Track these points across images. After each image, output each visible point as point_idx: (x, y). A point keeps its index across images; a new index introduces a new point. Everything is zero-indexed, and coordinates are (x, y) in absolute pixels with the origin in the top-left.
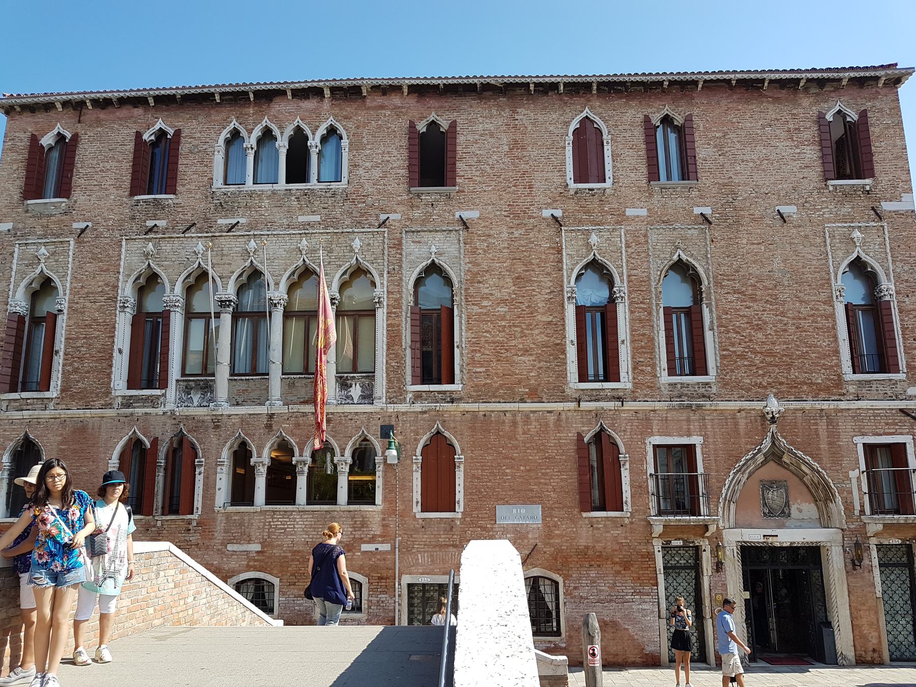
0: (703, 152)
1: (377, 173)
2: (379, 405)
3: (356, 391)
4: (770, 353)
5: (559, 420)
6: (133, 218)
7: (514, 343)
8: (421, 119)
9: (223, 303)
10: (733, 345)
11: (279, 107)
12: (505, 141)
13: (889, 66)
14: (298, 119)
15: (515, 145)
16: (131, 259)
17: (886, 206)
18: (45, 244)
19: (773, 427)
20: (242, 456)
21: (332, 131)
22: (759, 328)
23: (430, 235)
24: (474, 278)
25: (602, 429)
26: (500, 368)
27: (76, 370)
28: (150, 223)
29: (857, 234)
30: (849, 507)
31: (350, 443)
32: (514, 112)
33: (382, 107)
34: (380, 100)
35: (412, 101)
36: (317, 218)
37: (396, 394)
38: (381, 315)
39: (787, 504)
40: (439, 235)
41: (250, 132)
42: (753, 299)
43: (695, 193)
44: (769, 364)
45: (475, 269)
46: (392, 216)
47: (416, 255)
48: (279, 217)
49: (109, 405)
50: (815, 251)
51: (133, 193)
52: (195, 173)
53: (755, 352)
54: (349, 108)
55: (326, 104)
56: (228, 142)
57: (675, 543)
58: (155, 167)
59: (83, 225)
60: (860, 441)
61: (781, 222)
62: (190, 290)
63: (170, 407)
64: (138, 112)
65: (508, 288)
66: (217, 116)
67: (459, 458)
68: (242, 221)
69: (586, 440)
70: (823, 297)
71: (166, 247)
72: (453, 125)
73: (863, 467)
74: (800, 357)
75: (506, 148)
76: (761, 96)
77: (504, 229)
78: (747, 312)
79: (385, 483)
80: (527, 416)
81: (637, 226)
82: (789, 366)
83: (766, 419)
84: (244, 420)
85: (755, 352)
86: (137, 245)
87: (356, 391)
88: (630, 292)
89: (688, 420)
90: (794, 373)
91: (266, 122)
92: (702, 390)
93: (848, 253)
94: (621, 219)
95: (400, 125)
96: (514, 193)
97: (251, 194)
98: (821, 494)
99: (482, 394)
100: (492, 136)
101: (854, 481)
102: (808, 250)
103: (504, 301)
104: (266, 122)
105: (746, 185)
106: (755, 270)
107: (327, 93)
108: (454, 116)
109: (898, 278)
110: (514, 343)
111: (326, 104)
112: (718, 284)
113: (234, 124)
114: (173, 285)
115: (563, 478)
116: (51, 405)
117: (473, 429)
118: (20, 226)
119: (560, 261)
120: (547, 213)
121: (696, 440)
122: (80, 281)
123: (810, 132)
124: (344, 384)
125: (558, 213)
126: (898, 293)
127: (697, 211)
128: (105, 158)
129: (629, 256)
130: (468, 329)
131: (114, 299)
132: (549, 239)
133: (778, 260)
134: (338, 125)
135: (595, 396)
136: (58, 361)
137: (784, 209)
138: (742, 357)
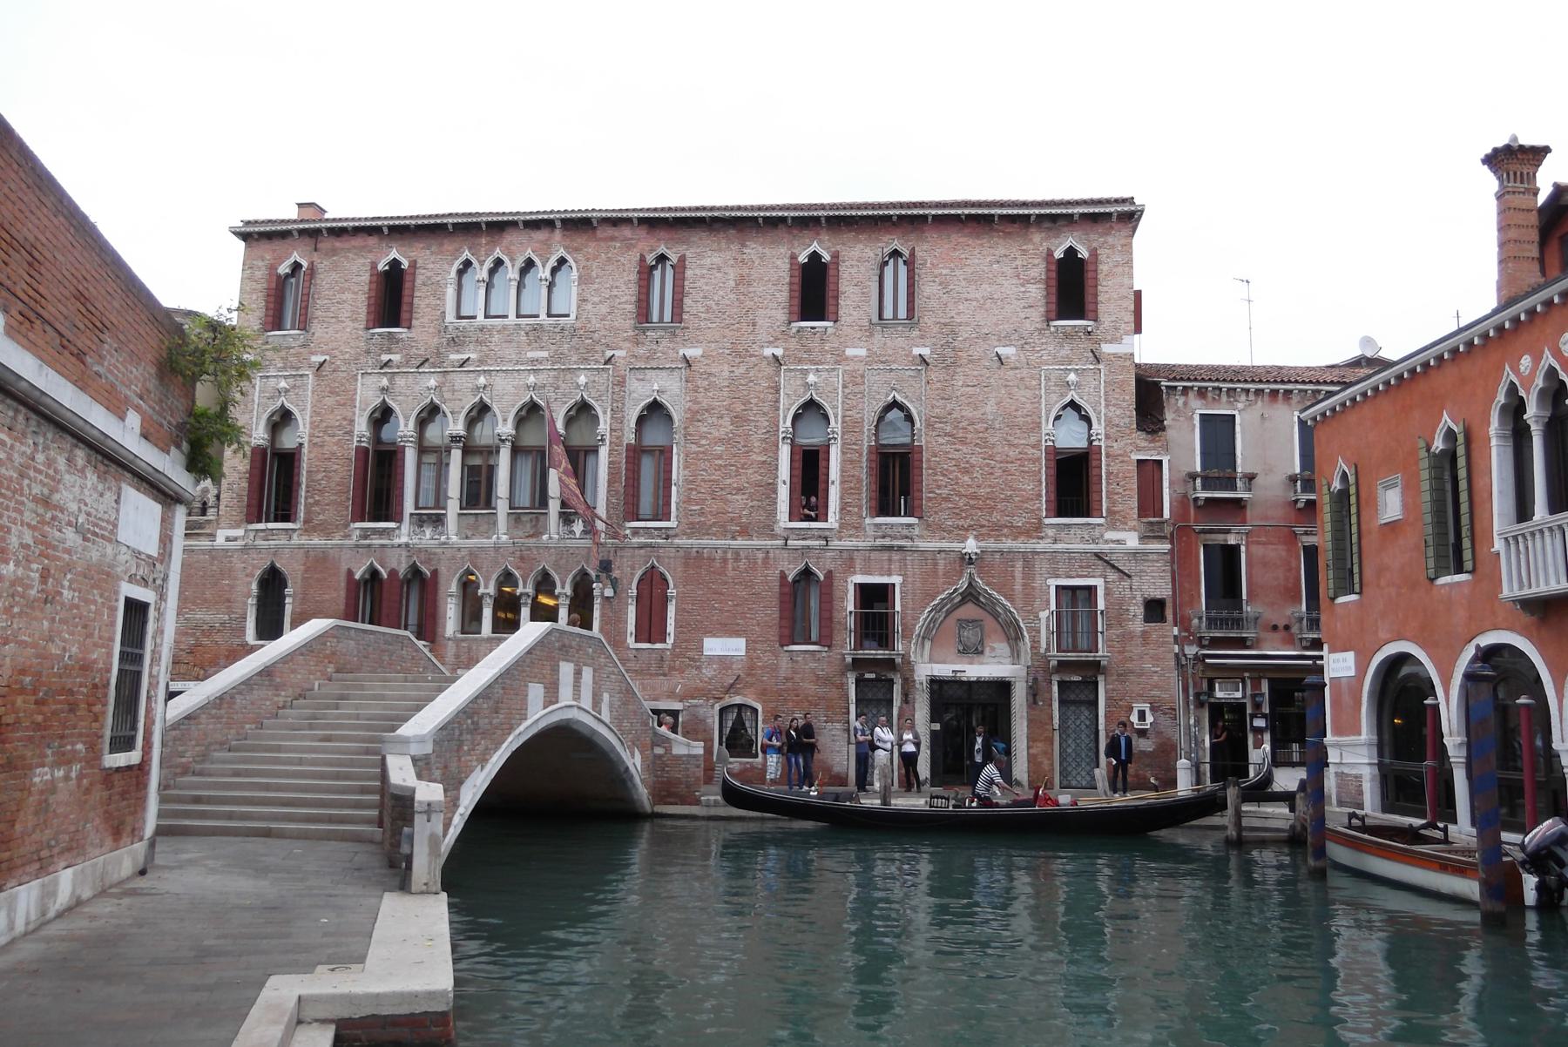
0: (928, 289)
1: (604, 309)
3: (578, 527)
4: (974, 497)
5: (767, 558)
6: (368, 352)
7: (729, 481)
8: (651, 251)
9: (455, 439)
10: (939, 487)
11: (511, 237)
12: (732, 276)
13: (1124, 201)
15: (741, 280)
16: (367, 395)
17: (1107, 348)
18: (285, 377)
19: (971, 569)
20: (468, 586)
21: (562, 261)
22: (966, 471)
23: (654, 373)
24: (694, 416)
26: (715, 506)
27: (317, 503)
28: (385, 358)
29: (1072, 377)
31: (570, 577)
32: (744, 245)
33: (613, 239)
35: (642, 232)
36: (545, 354)
38: (604, 452)
39: (982, 642)
40: (664, 373)
41: (482, 263)
42: (963, 441)
43: (916, 333)
44: (972, 507)
45: (696, 407)
46: (618, 353)
47: (640, 392)
49: (347, 536)
50: (1029, 393)
52: (428, 306)
53: (960, 495)
54: (580, 240)
55: (558, 234)
56: (461, 273)
57: (867, 676)
58: (391, 300)
60: (1053, 583)
62: (422, 423)
63: (404, 539)
64: (372, 241)
65: (726, 426)
66: (449, 246)
67: (672, 591)
68: (473, 356)
69: (790, 579)
70: (1033, 440)
71: (400, 382)
73: (1053, 607)
74: (1003, 500)
75: (732, 283)
76: (992, 229)
77: (726, 367)
78: (957, 455)
79: (602, 615)
80: (737, 552)
82: (993, 508)
83: (967, 560)
84: (473, 554)
85: (960, 495)
86: (370, 380)
87: (578, 527)
88: (843, 433)
89: (890, 560)
90: (996, 516)
91: (498, 253)
92: (905, 532)
93: (1063, 396)
94: (840, 358)
96: (738, 330)
98: (1013, 634)
99: (695, 529)
100: (719, 269)
101: (1043, 622)
102: (1023, 392)
105: (967, 324)
106: (968, 413)
107: (558, 224)
108: (682, 249)
109: (1109, 423)
110: (729, 481)
111: (558, 234)
112: (929, 425)
113: (466, 254)
114: (407, 419)
115: (768, 612)
116: (295, 536)
117: (686, 565)
119: (777, 401)
120: (768, 352)
121: (896, 580)
122: (318, 414)
123: (1039, 270)
124: (567, 518)
125: (779, 352)
126: (1107, 437)
127: (916, 351)
129: (845, 397)
130: (686, 467)
131: (350, 433)
132: (769, 378)
133: (992, 402)
134: (568, 257)
137: (1001, 350)
138: (947, 499)
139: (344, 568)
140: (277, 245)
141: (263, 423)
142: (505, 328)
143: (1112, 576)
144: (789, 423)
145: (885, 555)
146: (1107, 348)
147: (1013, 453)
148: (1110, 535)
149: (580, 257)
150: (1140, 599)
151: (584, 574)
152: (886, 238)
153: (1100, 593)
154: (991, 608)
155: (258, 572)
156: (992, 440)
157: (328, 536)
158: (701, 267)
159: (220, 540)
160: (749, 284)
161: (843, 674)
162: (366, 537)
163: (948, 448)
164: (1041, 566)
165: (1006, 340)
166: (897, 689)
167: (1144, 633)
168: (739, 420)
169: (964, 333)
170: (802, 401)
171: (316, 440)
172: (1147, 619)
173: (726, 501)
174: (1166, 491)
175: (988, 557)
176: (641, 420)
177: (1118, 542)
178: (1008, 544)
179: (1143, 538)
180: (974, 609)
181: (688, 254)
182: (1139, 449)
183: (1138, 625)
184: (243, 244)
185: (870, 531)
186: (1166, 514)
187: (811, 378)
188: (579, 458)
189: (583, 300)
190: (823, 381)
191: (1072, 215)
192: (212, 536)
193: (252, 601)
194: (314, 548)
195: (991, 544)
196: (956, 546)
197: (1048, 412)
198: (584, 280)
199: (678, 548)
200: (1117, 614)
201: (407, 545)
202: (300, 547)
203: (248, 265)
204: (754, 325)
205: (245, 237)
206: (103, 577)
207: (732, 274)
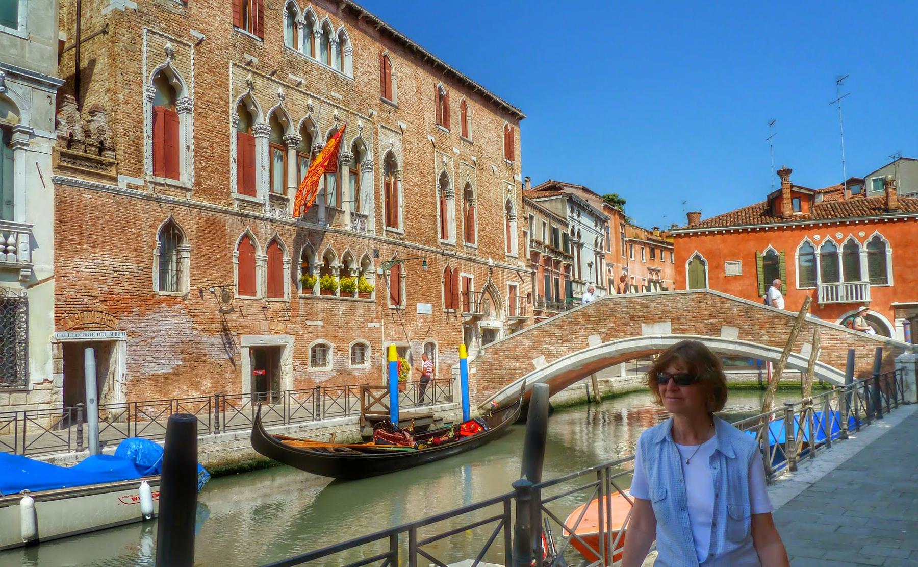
27: (204, 168)
28: (248, 57)
59: (200, 36)
118: (145, 10)
151: (366, 257)
155: (161, 225)
168: (422, 174)
171: (200, 110)
173: (421, 223)
193: (156, 252)
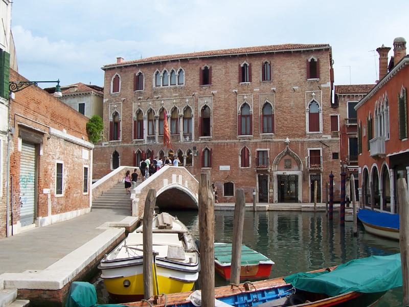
1: (192, 82)
2: (193, 141)
3: (188, 138)
4: (288, 127)
9: (156, 117)
11: (168, 65)
13: (326, 45)
14: (173, 68)
15: (227, 73)
16: (135, 107)
17: (322, 86)
21: (181, 70)
22: (286, 120)
24: (215, 109)
25: (245, 147)
28: (139, 98)
29: (314, 94)
30: (304, 165)
33: (194, 63)
34: (193, 61)
35: (201, 61)
37: (197, 139)
38: (193, 119)
39: (291, 165)
41: (161, 72)
42: (285, 112)
43: (272, 84)
47: (202, 103)
48: (169, 95)
50: (302, 99)
51: (134, 90)
54: (185, 64)
55: (179, 63)
56: (156, 75)
58: (138, 83)
59: (124, 99)
60: (309, 149)
61: (293, 91)
62: (149, 114)
63: (146, 143)
64: (135, 68)
70: (303, 111)
71: (143, 104)
72: (211, 67)
77: (223, 95)
78: (283, 116)
80: (227, 144)
81: (255, 94)
82: (293, 130)
83: (286, 144)
86: (136, 103)
87: (188, 138)
90: (294, 132)
91: (165, 69)
94: (252, 91)
95: (198, 67)
97: (162, 89)
98: (299, 164)
99: (217, 138)
103: (223, 115)
104: (165, 69)
105: (285, 81)
108: (211, 64)
109: (323, 106)
111: (179, 63)
112: (276, 109)
120: (234, 91)
121: (268, 149)
123: (304, 65)
124: (185, 136)
125: (237, 91)
126: (323, 110)
127: (272, 89)
128: (127, 81)
135: (244, 138)
136: (121, 132)
137: (294, 88)
139: (132, 151)
140: (112, 71)
141: (111, 116)
142: (167, 88)
143: (324, 147)
144: (240, 109)
145: (265, 143)
146: (322, 86)
147: (298, 115)
148: (324, 136)
149: (185, 69)
150: (331, 153)
152: (264, 58)
153: (321, 151)
154: (293, 156)
155: (112, 153)
156: (292, 112)
157: (128, 143)
158: (216, 69)
159: (103, 145)
160: (228, 73)
161: (255, 174)
162: (137, 143)
163: (281, 114)
164: (306, 146)
165: (296, 85)
166: (269, 178)
167: (332, 162)
168: (227, 109)
169: (285, 83)
170: (242, 104)
172: (333, 158)
173: (224, 131)
174: (339, 124)
175: (292, 143)
176: (202, 110)
177: (326, 138)
178: (297, 139)
179: (332, 137)
180: (289, 158)
181: (212, 66)
182: (332, 113)
183: (331, 160)
184: (104, 71)
185: (261, 137)
186: (339, 130)
187: (245, 97)
188: (187, 119)
189: (186, 80)
190: (247, 98)
191: (312, 50)
192: (101, 145)
193: (112, 160)
194: (125, 146)
195: (293, 140)
196: (283, 140)
197: (307, 103)
198: (187, 75)
199: (213, 143)
200: (325, 158)
201: (146, 145)
202: (121, 146)
203: (106, 77)
204: (230, 84)
205: (105, 70)
206: (80, 165)
207: (224, 70)
